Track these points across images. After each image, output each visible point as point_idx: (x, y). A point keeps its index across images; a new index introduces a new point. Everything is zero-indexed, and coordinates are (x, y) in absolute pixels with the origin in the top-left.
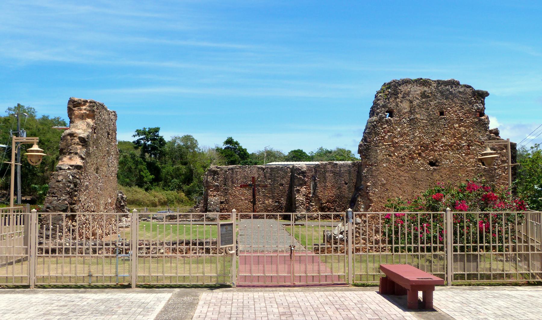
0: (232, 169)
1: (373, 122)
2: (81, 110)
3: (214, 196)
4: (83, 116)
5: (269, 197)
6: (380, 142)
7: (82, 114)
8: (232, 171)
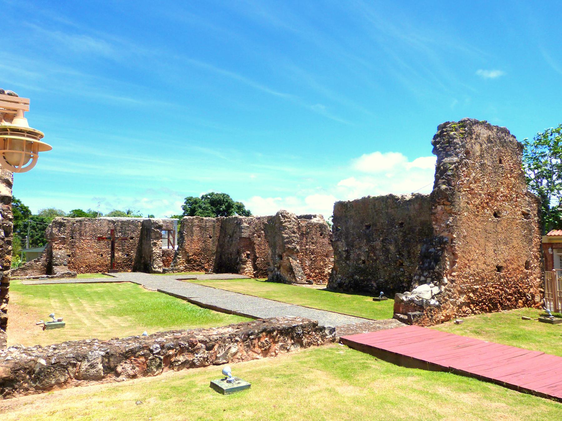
0: (80, 221)
3: (60, 249)
5: (119, 250)
8: (81, 224)
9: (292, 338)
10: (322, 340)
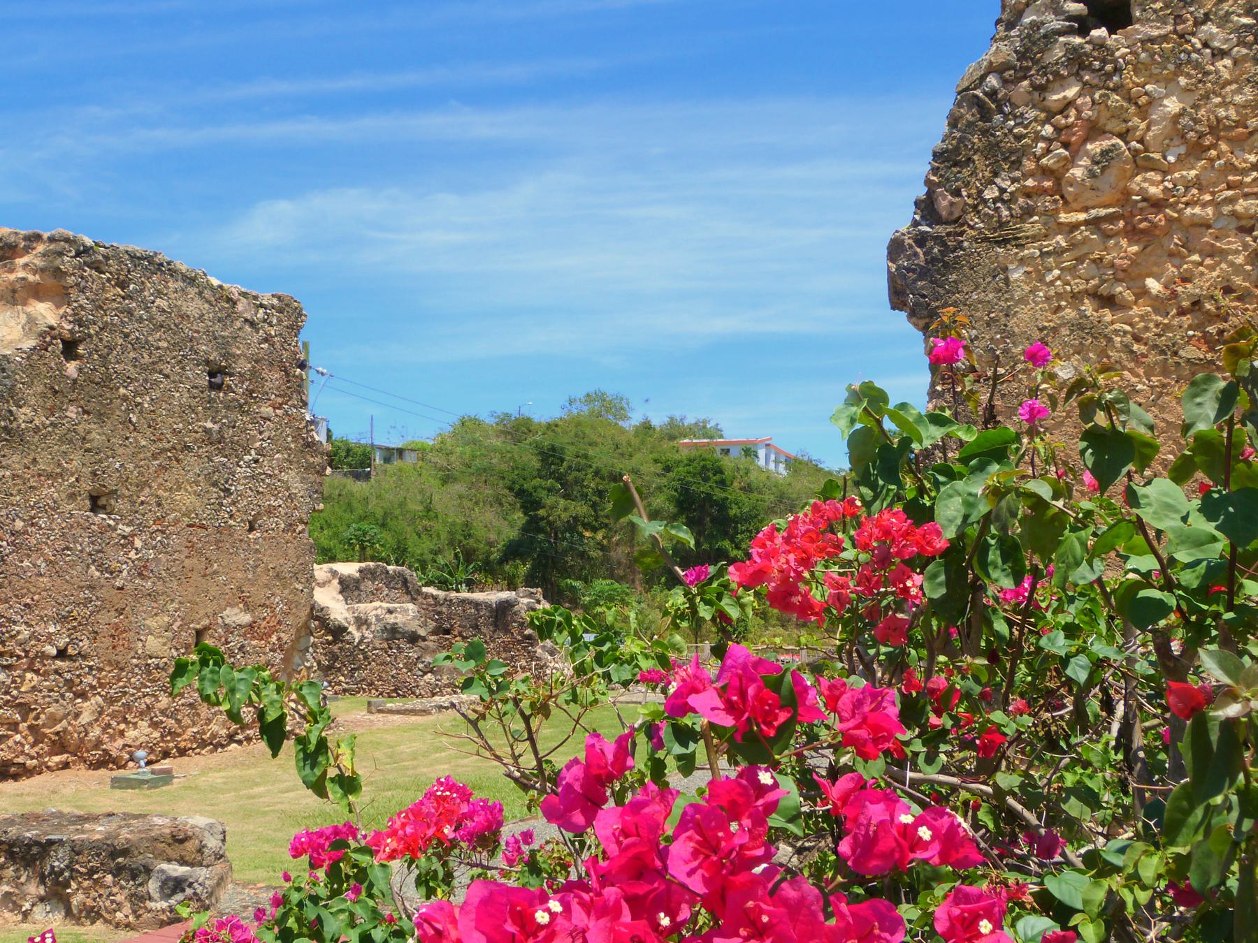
1: (982, 78)
2: (12, 271)
4: (14, 291)
6: (1028, 212)
7: (12, 283)
9: (42, 880)
10: (134, 912)
